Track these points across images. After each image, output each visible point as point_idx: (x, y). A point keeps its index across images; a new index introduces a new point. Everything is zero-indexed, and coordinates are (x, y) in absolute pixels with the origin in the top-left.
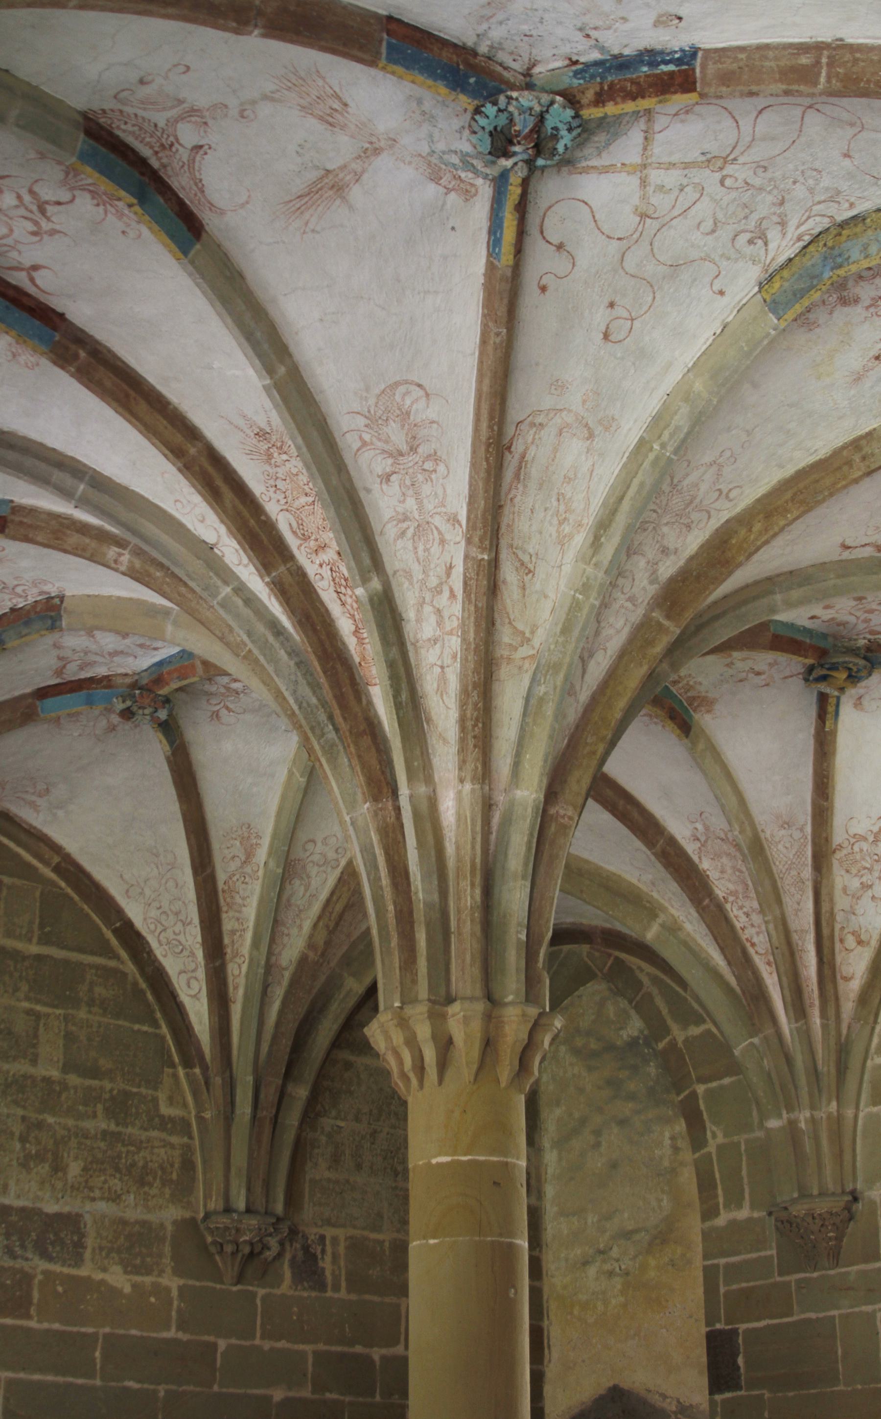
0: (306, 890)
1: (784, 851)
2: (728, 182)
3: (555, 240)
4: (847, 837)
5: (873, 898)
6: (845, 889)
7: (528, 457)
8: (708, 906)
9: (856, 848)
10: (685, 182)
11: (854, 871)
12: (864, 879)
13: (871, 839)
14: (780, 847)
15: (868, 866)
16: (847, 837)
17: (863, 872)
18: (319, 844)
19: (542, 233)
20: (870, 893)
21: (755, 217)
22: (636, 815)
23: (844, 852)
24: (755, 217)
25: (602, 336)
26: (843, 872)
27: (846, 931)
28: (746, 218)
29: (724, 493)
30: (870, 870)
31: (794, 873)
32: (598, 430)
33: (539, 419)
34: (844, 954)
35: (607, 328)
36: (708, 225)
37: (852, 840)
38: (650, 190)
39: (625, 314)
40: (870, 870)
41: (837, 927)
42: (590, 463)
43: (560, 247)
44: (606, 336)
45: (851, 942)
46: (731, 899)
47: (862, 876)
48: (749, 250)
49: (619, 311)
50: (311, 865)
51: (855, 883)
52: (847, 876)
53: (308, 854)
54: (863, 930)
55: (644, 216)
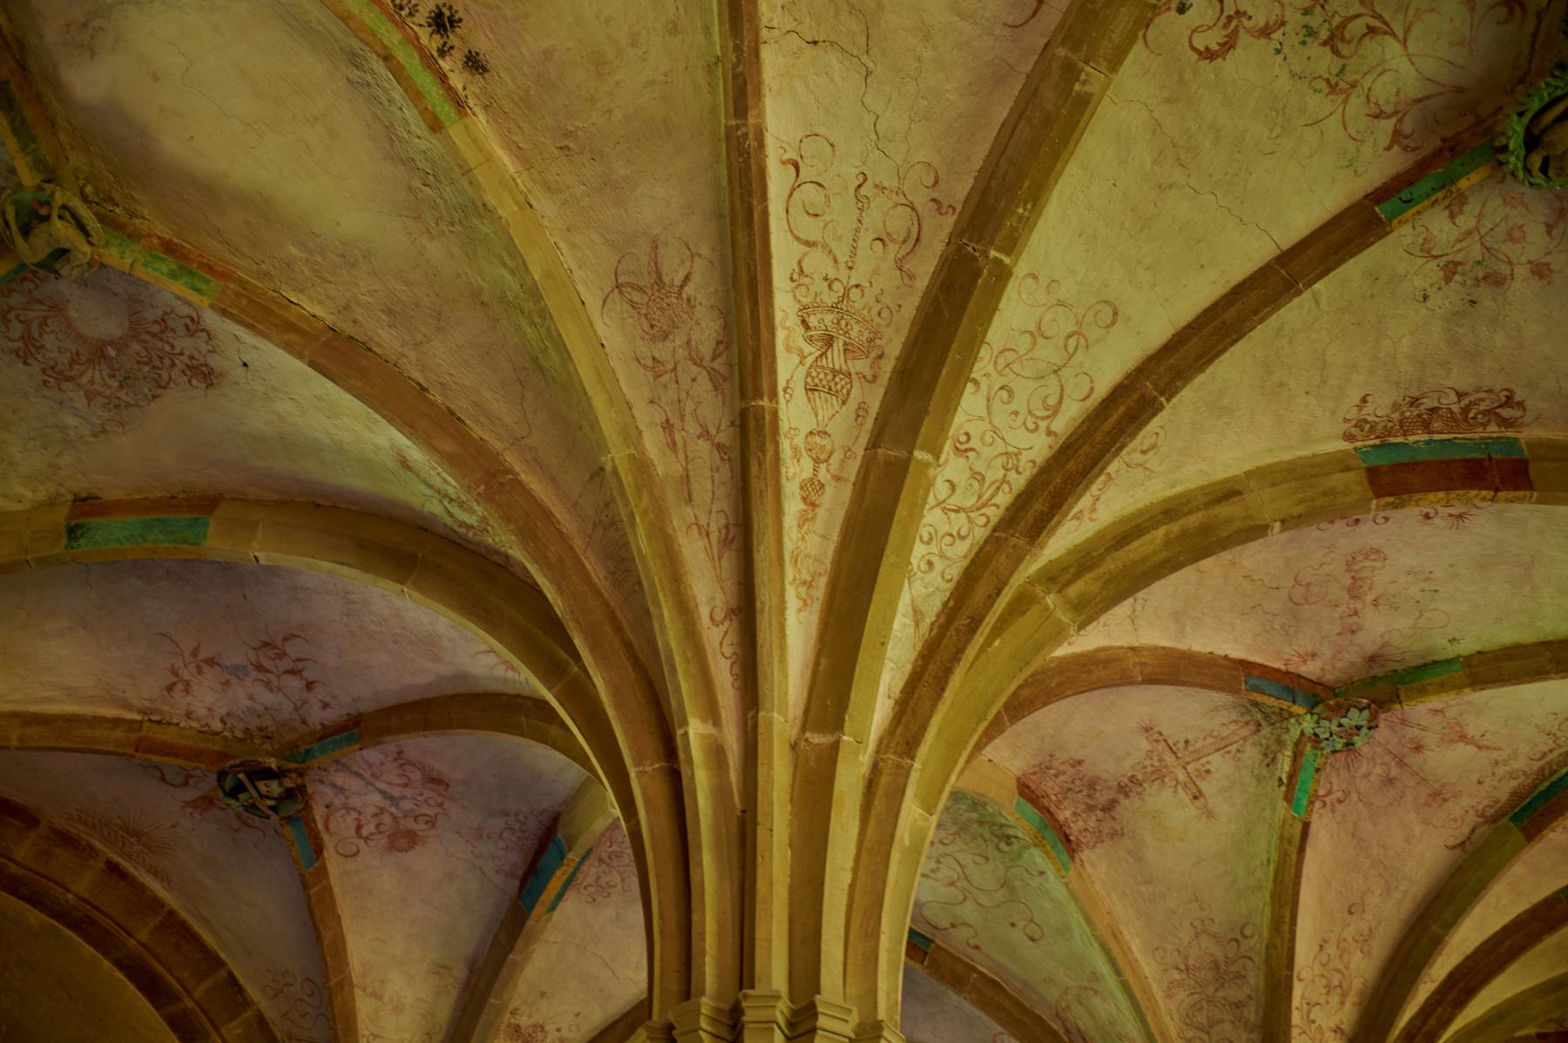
2: (945, 841)
3: (947, 925)
7: (1082, 1028)
10: (934, 860)
19: (937, 928)
21: (987, 835)
24: (987, 835)
25: (1031, 942)
28: (985, 841)
29: (1239, 937)
32: (1095, 985)
33: (1064, 1005)
35: (1027, 936)
36: (979, 859)
38: (932, 875)
39: (1026, 923)
42: (1113, 1006)
43: (953, 926)
44: (1032, 940)
48: (1015, 847)
49: (1021, 924)
55: (952, 884)
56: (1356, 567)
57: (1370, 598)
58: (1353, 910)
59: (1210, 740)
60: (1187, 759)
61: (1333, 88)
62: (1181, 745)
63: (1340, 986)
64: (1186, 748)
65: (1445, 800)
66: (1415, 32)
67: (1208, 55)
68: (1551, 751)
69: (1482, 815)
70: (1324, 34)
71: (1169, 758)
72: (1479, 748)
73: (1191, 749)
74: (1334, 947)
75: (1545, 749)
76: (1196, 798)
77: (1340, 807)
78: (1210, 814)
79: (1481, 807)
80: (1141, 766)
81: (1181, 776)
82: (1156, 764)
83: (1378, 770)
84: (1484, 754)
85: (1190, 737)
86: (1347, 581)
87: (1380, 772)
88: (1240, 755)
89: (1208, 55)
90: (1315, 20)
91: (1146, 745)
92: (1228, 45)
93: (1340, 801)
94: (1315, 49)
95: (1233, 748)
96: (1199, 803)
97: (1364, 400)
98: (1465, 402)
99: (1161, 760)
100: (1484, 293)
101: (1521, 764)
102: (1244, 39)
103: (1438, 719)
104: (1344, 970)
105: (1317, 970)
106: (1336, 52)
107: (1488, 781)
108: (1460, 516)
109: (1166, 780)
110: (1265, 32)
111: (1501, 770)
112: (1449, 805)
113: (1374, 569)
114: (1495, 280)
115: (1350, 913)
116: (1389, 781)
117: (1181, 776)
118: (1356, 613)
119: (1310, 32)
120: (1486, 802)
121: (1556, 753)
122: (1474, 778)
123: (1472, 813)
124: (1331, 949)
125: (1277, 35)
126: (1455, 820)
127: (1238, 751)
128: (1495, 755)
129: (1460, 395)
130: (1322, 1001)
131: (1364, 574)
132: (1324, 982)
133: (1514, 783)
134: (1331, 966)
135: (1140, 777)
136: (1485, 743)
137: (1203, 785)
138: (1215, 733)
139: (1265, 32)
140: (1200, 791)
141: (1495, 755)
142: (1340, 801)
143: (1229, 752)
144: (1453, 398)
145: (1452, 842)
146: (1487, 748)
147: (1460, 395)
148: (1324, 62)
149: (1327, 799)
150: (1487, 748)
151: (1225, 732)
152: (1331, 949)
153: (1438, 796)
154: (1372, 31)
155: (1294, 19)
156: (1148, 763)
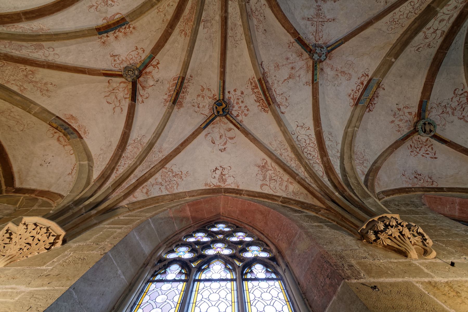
0: (30, 52)
1: (153, 157)
4: (170, 168)
5: (160, 188)
6: (156, 179)
8: (119, 151)
9: (169, 173)
11: (163, 178)
12: (162, 182)
13: (174, 175)
14: (154, 155)
15: (166, 180)
16: (170, 168)
17: (164, 180)
18: (53, 52)
20: (161, 186)
22: (131, 121)
23: (166, 171)
26: (160, 175)
27: (146, 187)
30: (166, 182)
31: (150, 163)
34: (140, 191)
37: (170, 170)
40: (166, 182)
41: (145, 184)
45: (145, 191)
46: (125, 158)
47: (163, 181)
50: (43, 52)
51: (160, 180)
52: (160, 177)
53: (48, 49)
54: (150, 192)
56: (348, 75)
57: (339, 74)
58: (265, 31)
59: (320, 30)
60: (318, 23)
61: (439, 104)
62: (323, 24)
63: (255, 13)
64: (321, 24)
65: (275, 67)
66: (439, 117)
67: (455, 90)
68: (276, 93)
69: (266, 73)
70: (446, 106)
71: (321, 20)
72: (285, 80)
73: (320, 25)
74: (262, 20)
75: (277, 92)
76: (308, 19)
77: (288, 45)
78: (303, 19)
79: (268, 74)
80: (323, 13)
81: (314, 19)
82: (321, 17)
83: (291, 58)
84: (283, 80)
85: (324, 27)
86: (346, 72)
87: (291, 58)
88: (312, 34)
89: (455, 90)
90: (449, 105)
91: (328, 17)
92: (454, 93)
93: (289, 46)
94: (446, 104)
95: (315, 34)
96: (307, 18)
97: (384, 89)
98: (373, 104)
99: (321, 18)
100: (393, 113)
101: (275, 86)
102: (453, 95)
103: (298, 75)
104: (257, 17)
105: (262, 11)
106: (444, 106)
107: (275, 78)
108: (350, 96)
109: (316, 16)
110: (452, 99)
111: (276, 82)
112: (274, 67)
113: (346, 78)
114: (395, 115)
115: (265, 30)
116: (287, 59)
117: (314, 19)
118: (336, 71)
119: (448, 104)
120: (269, 75)
121: (275, 94)
122: (277, 76)
123: (268, 71)
124: (262, 19)
125: (450, 100)
126: (269, 67)
127: (313, 34)
128: (281, 82)
129: (375, 104)
130: (256, 5)
131: (346, 76)
132: (258, 10)
133: (270, 83)
134: (259, 15)
135: (320, 11)
136: (286, 81)
137: (310, 22)
138: (321, 32)
139: (452, 99)
140: (309, 21)
141: (281, 82)
142: (289, 46)
143: (314, 32)
144: (375, 103)
145: (263, 63)
146: (284, 81)
147: (375, 104)
148: (443, 104)
149: (291, 44)
150: (284, 81)
151: (320, 34)
152: (262, 19)
153: (277, 66)
154: (443, 111)
155: (450, 103)
156: (323, 15)
